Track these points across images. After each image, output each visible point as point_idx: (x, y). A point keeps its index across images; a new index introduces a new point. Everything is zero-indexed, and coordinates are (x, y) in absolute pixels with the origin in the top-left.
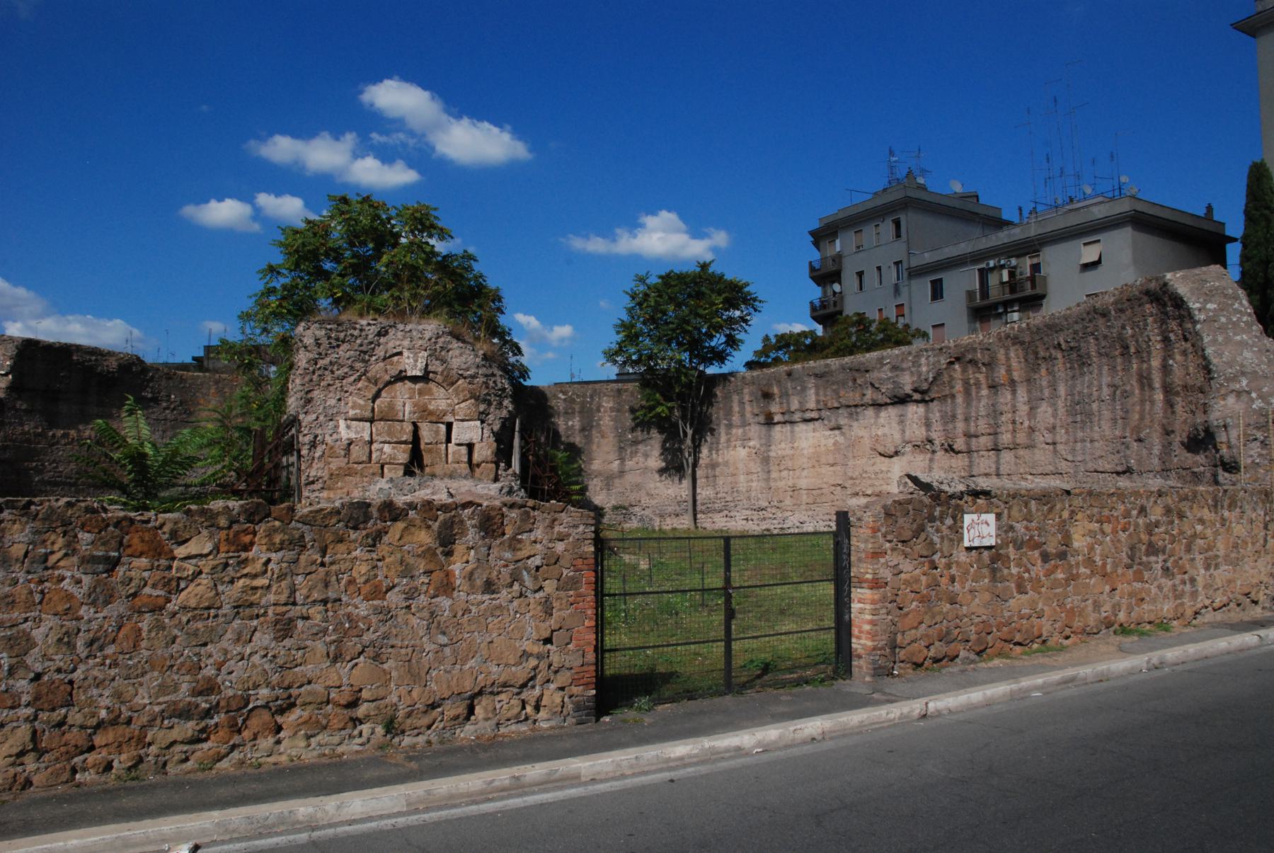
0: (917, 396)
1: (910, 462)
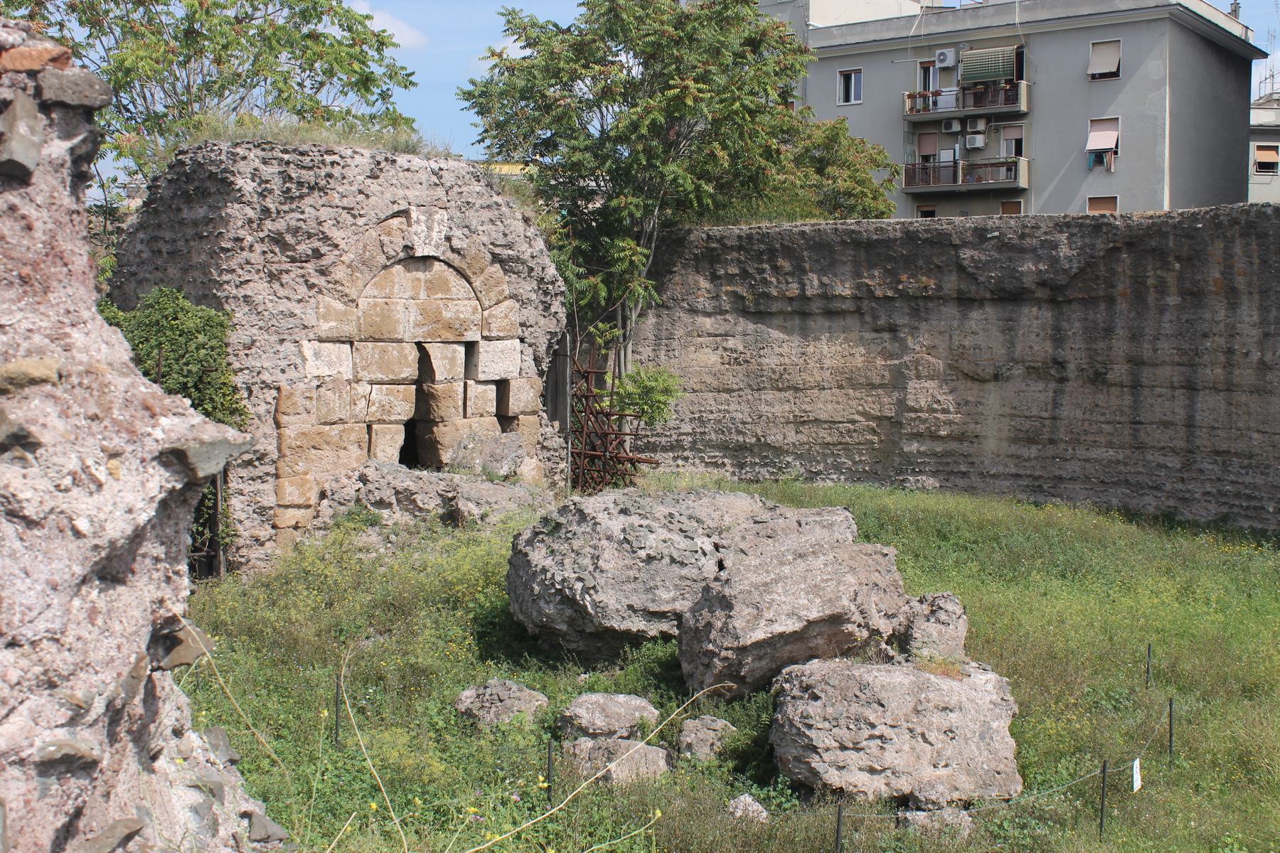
0: (1041, 293)
1: (1018, 393)
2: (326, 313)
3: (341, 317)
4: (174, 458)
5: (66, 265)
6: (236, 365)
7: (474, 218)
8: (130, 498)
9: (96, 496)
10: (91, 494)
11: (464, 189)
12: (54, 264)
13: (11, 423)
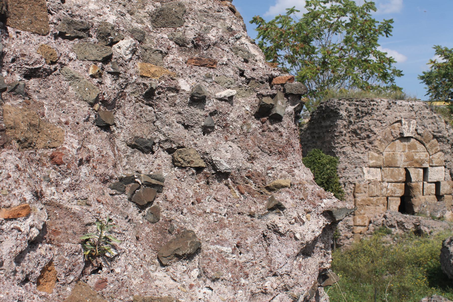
2: (372, 157)
3: (377, 159)
4: (328, 214)
5: (293, 147)
6: (340, 176)
7: (426, 122)
8: (314, 227)
9: (302, 226)
10: (301, 225)
11: (422, 112)
12: (289, 147)
13: (276, 201)
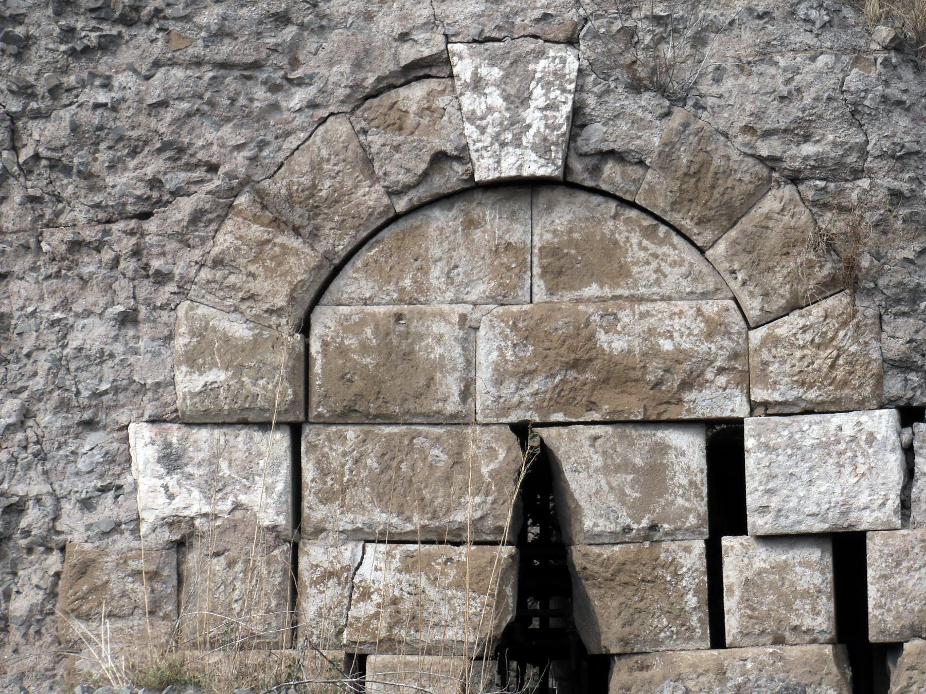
3: (235, 355)
